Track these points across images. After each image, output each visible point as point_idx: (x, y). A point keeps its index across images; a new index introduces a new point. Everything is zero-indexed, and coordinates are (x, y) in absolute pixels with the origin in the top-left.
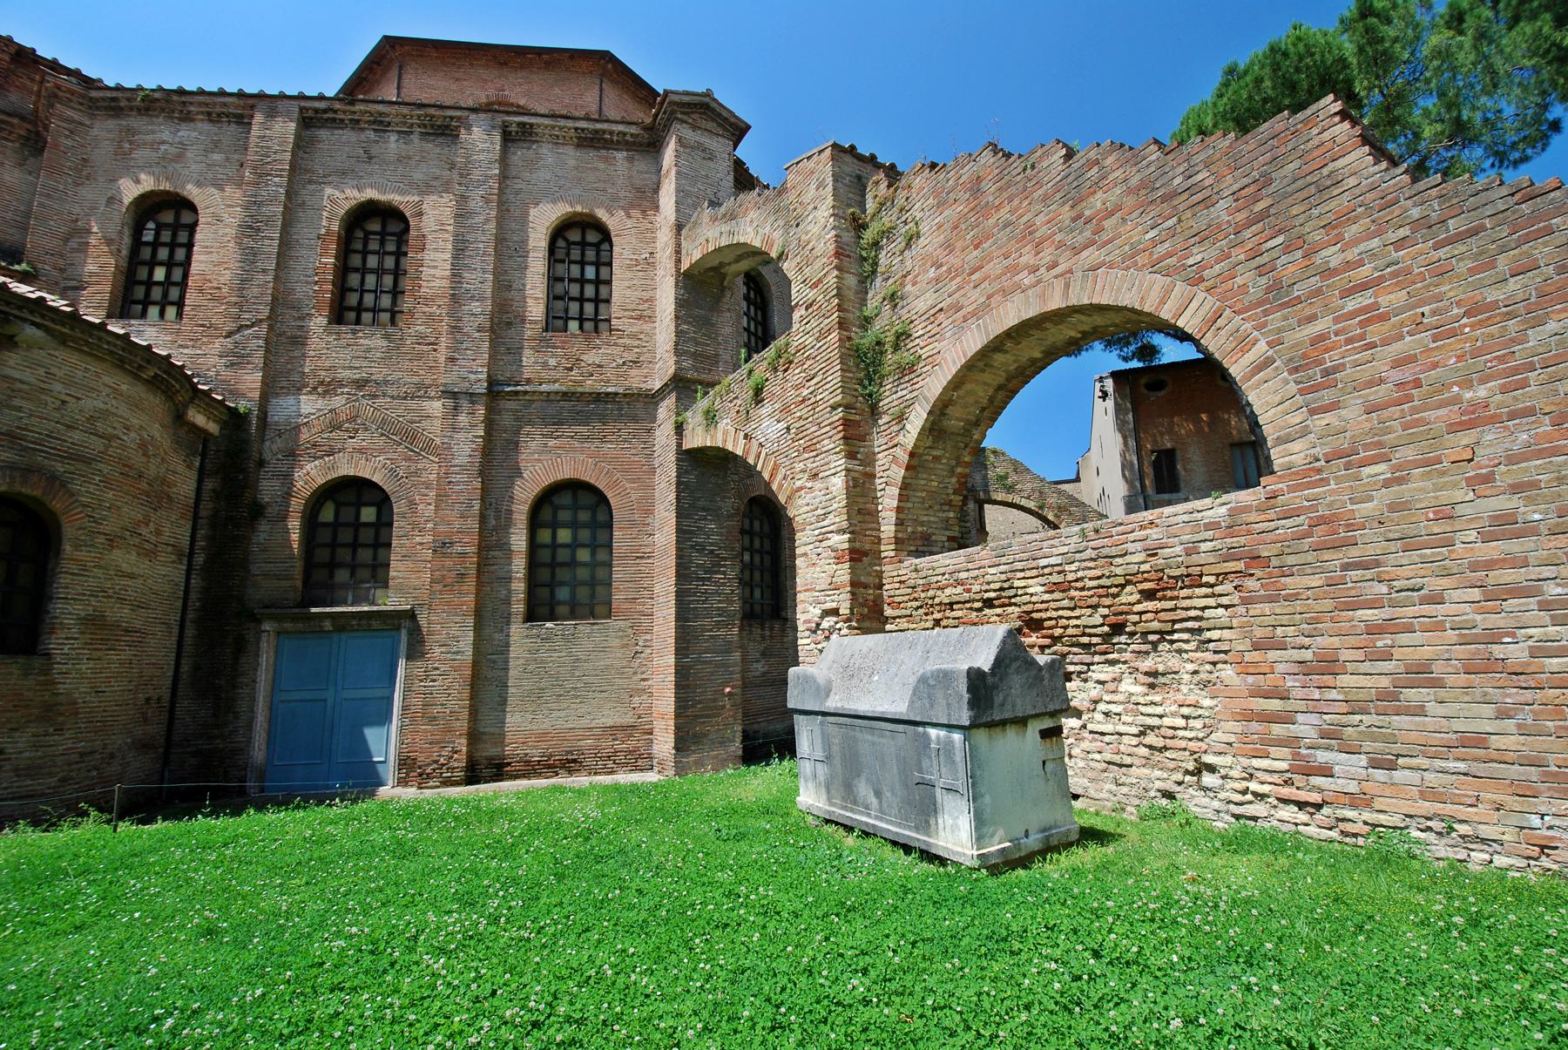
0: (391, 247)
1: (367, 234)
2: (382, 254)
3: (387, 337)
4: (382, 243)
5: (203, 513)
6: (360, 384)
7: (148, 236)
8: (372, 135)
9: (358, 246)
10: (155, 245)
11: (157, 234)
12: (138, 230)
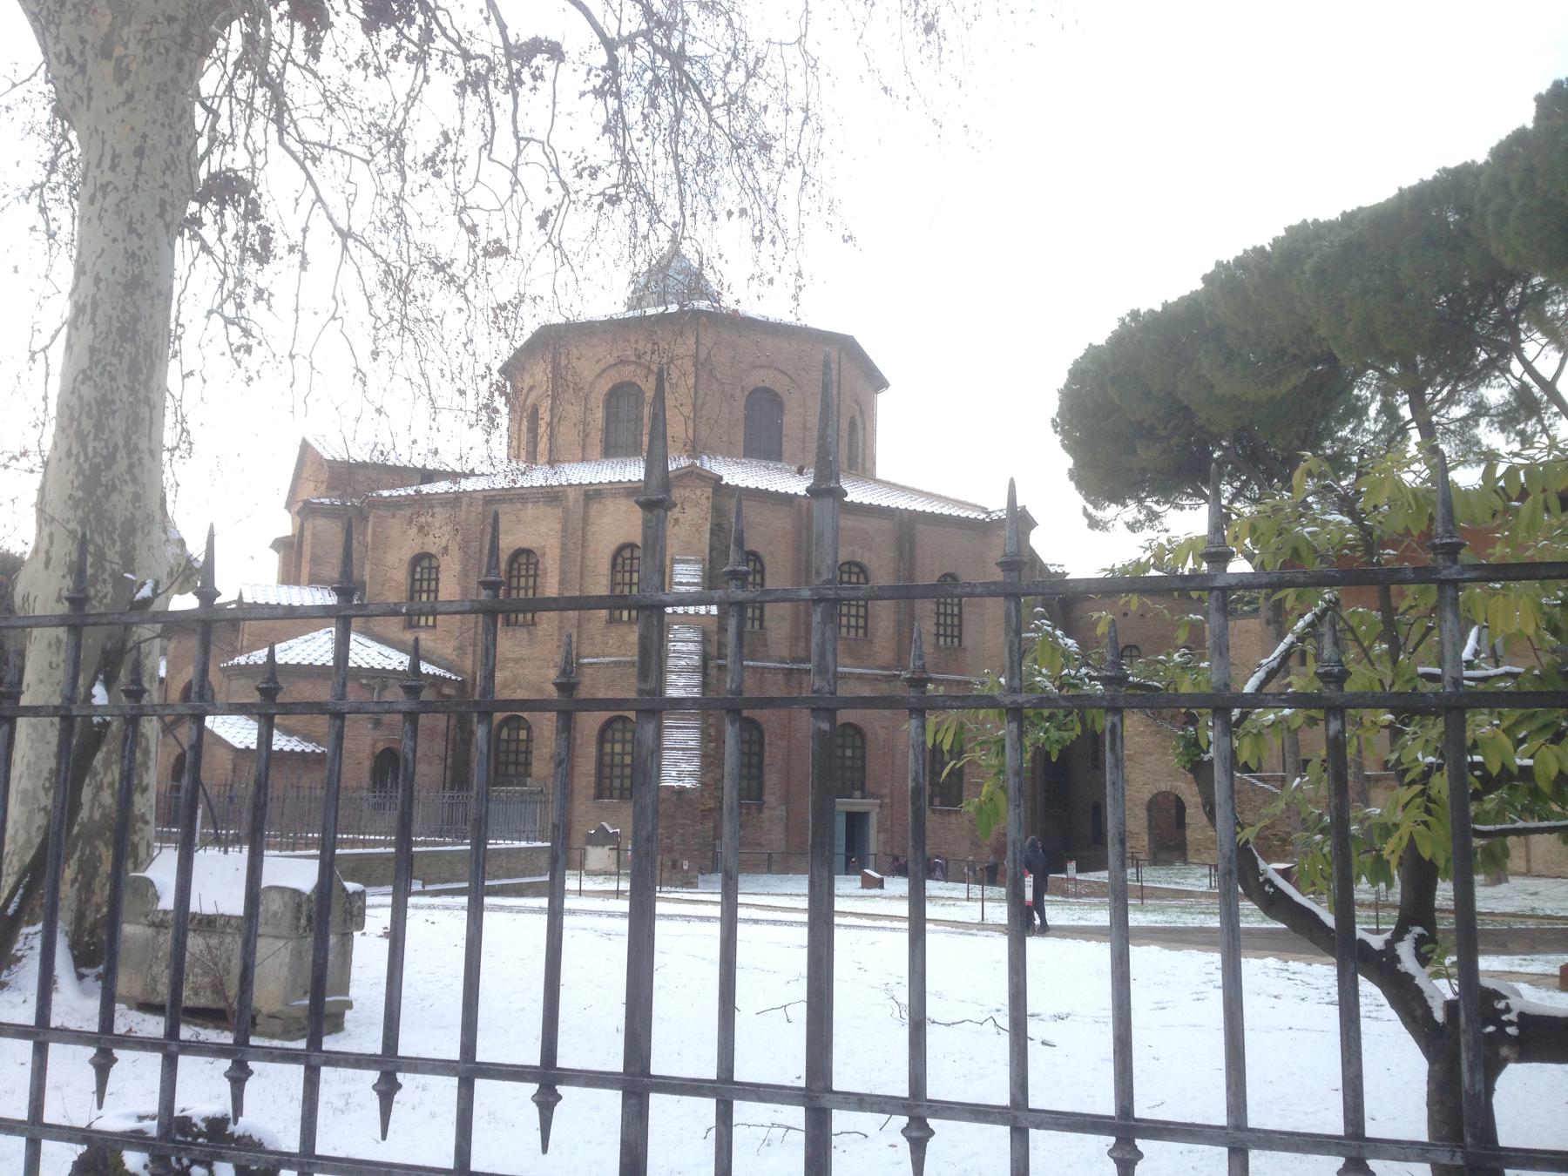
0: (532, 572)
1: (520, 565)
2: (527, 576)
3: (529, 633)
4: (527, 570)
5: (451, 737)
6: (516, 661)
7: (418, 576)
8: (519, 506)
9: (515, 573)
10: (421, 580)
11: (422, 573)
12: (413, 572)
